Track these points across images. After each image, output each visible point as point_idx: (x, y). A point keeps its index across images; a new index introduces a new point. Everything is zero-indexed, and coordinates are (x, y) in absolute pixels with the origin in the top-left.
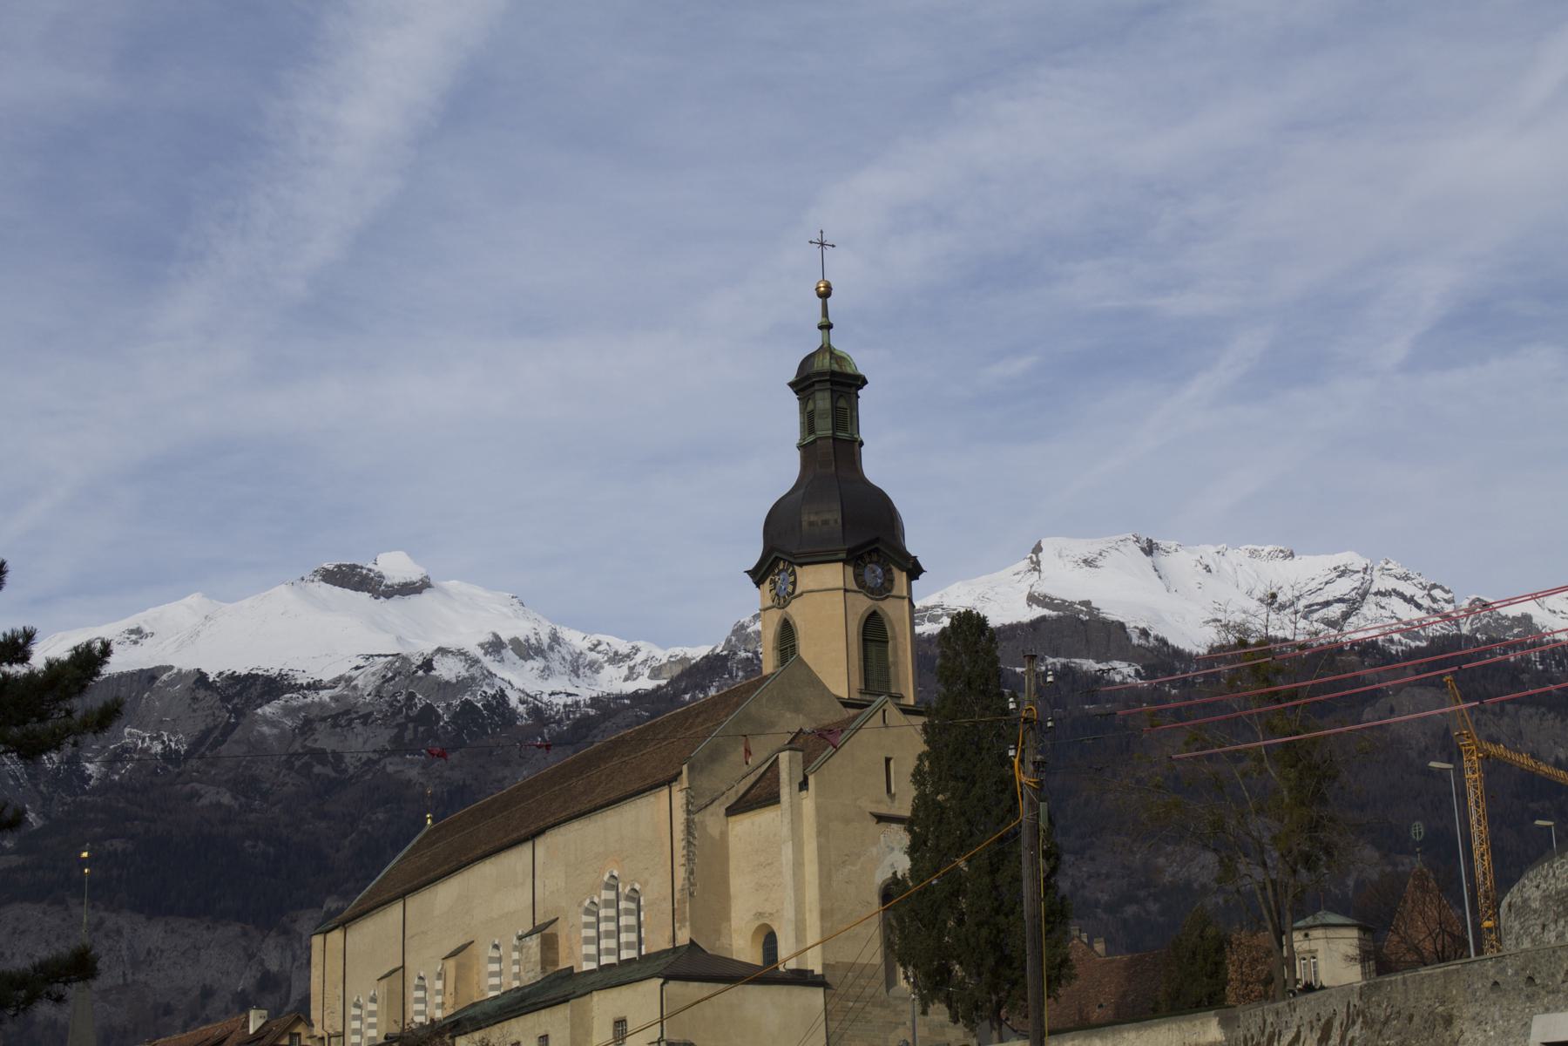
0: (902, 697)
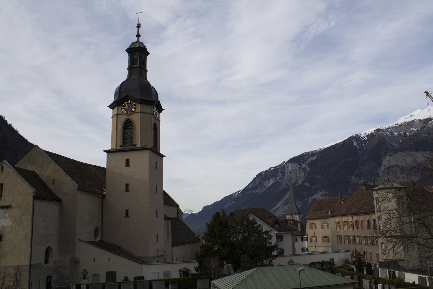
0: (136, 145)
